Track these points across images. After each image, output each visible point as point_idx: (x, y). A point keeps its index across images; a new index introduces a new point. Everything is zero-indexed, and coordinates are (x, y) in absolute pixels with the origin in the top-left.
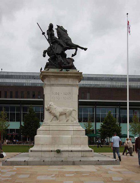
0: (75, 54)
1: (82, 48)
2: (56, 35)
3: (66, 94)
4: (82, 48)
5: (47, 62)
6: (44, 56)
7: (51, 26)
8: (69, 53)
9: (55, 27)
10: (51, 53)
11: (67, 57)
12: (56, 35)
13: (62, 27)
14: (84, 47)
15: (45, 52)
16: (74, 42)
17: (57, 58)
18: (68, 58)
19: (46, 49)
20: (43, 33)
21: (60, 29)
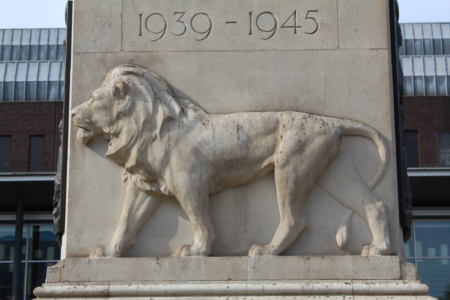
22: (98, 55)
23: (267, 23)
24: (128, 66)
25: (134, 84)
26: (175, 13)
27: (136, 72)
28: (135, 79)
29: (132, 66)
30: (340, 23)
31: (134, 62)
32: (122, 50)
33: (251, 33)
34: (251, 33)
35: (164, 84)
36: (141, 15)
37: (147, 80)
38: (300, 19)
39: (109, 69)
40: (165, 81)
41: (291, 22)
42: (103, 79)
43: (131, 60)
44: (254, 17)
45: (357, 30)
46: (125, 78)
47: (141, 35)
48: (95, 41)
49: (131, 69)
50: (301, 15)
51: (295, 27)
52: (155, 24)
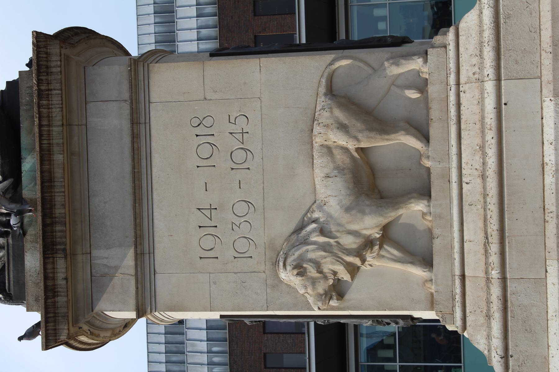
3: (206, 151)
22: (269, 291)
23: (239, 156)
24: (278, 266)
25: (294, 260)
26: (233, 229)
27: (283, 259)
28: (289, 260)
29: (278, 263)
30: (238, 97)
31: (274, 262)
32: (264, 272)
33: (248, 168)
34: (248, 168)
35: (292, 237)
36: (235, 258)
37: (290, 250)
39: (281, 281)
40: (290, 236)
41: (239, 136)
42: (289, 286)
43: (273, 264)
44: (235, 166)
45: (245, 83)
46: (289, 268)
47: (251, 257)
48: (257, 294)
49: (281, 264)
51: (243, 133)
52: (242, 245)
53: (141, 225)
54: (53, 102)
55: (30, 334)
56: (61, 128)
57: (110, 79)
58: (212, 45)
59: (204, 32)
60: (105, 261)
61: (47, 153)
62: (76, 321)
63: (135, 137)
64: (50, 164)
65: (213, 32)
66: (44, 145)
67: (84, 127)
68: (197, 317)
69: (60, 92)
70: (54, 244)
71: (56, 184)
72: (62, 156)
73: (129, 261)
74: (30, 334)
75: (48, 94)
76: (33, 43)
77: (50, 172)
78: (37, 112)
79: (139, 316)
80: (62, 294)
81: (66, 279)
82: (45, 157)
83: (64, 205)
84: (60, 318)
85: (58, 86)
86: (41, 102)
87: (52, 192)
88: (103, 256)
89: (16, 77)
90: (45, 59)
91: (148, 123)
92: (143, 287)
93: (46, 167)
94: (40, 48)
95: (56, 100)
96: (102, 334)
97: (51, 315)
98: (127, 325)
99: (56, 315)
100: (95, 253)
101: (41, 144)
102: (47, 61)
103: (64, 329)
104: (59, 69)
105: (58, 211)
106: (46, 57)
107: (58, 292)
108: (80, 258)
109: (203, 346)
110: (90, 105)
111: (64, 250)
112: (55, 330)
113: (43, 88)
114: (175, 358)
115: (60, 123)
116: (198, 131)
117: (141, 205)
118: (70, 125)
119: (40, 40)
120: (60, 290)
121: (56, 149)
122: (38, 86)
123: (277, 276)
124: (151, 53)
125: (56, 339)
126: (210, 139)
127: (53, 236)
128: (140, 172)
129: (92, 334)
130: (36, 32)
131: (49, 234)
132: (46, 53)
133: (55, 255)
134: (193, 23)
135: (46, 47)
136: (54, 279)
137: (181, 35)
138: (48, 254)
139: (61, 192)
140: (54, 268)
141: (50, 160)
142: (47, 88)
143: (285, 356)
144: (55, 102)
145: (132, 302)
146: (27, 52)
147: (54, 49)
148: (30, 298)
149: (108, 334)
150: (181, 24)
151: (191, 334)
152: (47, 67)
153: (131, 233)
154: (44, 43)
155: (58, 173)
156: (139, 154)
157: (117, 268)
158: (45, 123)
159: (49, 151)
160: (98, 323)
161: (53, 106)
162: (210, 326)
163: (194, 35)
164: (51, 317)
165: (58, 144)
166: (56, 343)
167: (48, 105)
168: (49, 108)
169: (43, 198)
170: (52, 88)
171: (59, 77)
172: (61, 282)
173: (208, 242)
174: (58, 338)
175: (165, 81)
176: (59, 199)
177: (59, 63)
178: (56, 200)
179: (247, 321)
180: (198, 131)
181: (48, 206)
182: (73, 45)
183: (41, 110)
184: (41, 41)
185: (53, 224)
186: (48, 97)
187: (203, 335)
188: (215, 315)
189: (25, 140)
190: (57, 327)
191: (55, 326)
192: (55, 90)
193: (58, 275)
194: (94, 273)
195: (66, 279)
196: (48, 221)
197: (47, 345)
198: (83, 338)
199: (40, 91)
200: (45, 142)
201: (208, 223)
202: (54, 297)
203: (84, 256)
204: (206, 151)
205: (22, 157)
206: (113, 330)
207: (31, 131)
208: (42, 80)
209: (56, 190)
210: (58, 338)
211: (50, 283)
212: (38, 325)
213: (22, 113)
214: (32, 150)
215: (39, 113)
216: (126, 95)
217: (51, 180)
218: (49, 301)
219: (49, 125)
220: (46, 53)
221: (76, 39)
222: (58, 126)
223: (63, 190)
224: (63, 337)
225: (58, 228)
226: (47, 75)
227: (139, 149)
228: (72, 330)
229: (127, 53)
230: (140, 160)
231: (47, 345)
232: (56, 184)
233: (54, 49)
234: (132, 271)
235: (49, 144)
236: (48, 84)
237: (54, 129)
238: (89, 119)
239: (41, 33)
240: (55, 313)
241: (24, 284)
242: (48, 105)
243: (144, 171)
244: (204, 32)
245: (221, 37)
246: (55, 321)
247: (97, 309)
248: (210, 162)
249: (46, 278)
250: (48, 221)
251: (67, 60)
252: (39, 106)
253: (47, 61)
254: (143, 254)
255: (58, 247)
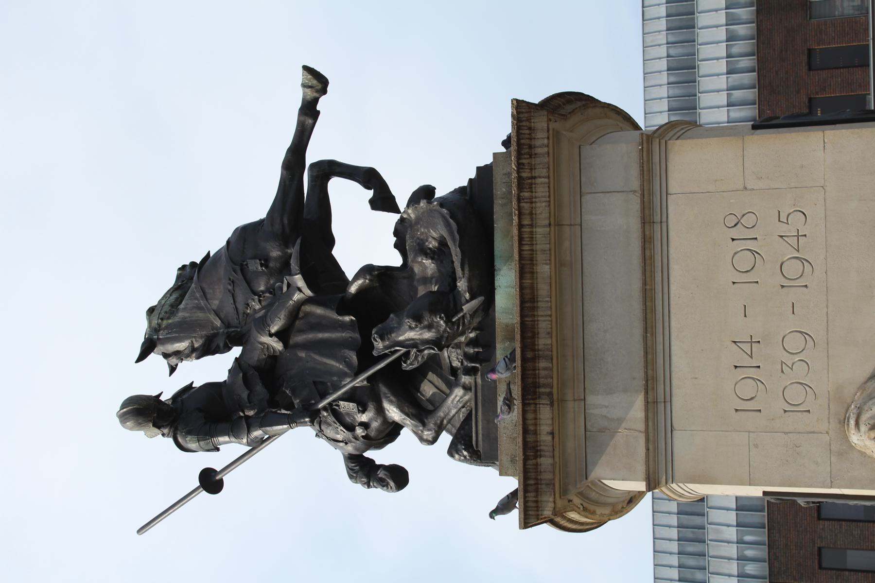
0: (369, 178)
1: (309, 111)
2: (215, 368)
3: (745, 261)
4: (309, 111)
5: (452, 451)
6: (398, 477)
7: (144, 411)
8: (362, 240)
9: (160, 380)
10: (364, 418)
11: (395, 260)
12: (215, 368)
13: (151, 311)
14: (296, 98)
15: (363, 470)
16: (256, 201)
17: (398, 361)
18: (400, 245)
19: (333, 459)
20: (210, 481)
21: (171, 326)
22: (833, 459)
23: (793, 268)
24: (848, 425)
25: (871, 418)
26: (782, 371)
27: (855, 416)
28: (865, 417)
29: (848, 421)
30: (793, 185)
31: (842, 418)
32: (827, 433)
33: (806, 286)
34: (806, 286)
35: (869, 384)
36: (785, 411)
37: (865, 403)
38: (783, 229)
39: (851, 447)
40: (866, 382)
41: (793, 241)
42: (863, 454)
43: (840, 423)
44: (786, 283)
45: (802, 166)
46: (863, 428)
47: (809, 411)
48: (816, 463)
49: (852, 422)
50: (783, 229)
51: (798, 236)
52: (795, 394)
53: (654, 362)
54: (537, 194)
55: (504, 507)
56: (548, 229)
57: (613, 163)
58: (750, 112)
59: (738, 94)
60: (604, 411)
61: (528, 262)
62: (564, 492)
63: (647, 241)
64: (532, 278)
65: (751, 94)
66: (526, 253)
67: (578, 228)
68: (724, 492)
69: (547, 180)
70: (536, 385)
71: (540, 304)
72: (548, 267)
73: (637, 411)
74: (504, 507)
75: (531, 184)
76: (513, 115)
77: (532, 288)
78: (516, 207)
79: (650, 488)
80: (547, 454)
81: (552, 433)
82: (526, 269)
83: (550, 334)
84: (543, 486)
85: (544, 172)
86: (522, 194)
87: (534, 316)
88: (601, 404)
89: (489, 160)
90: (527, 136)
91: (665, 222)
92: (656, 449)
93: (527, 282)
94: (521, 121)
95: (541, 191)
96: (599, 511)
97: (532, 482)
98: (632, 499)
99: (538, 481)
100: (591, 399)
101: (520, 251)
102: (530, 139)
103: (548, 502)
104: (546, 149)
105: (543, 342)
106: (530, 134)
107: (540, 450)
108: (570, 405)
109: (731, 533)
110: (587, 198)
111: (550, 394)
112: (537, 502)
113: (524, 175)
114: (691, 548)
115: (547, 222)
116: (734, 233)
117: (654, 334)
118: (559, 225)
119: (522, 110)
120: (543, 448)
121: (540, 257)
122: (518, 172)
123: (846, 439)
124: (670, 126)
125: (538, 515)
126: (751, 245)
127: (535, 374)
128: (653, 290)
129: (585, 509)
130: (517, 100)
131: (531, 372)
132: (530, 129)
133: (537, 401)
134: (722, 82)
135: (529, 120)
136: (535, 433)
137: (705, 100)
138: (528, 399)
139: (546, 316)
140: (536, 419)
141: (532, 273)
142: (529, 175)
143: (850, 553)
144: (540, 194)
145: (641, 468)
146: (506, 128)
147: (540, 122)
148: (504, 457)
149: (607, 511)
150: (705, 83)
151: (715, 516)
152: (530, 147)
153: (640, 374)
154: (526, 115)
155: (543, 290)
156: (653, 265)
157: (620, 421)
158: (526, 222)
159: (531, 260)
160: (593, 496)
161: (537, 200)
162: (743, 505)
163: (722, 99)
164: (531, 485)
165: (543, 251)
166: (538, 519)
167: (531, 198)
168: (532, 203)
169: (523, 324)
170: (537, 175)
171: (546, 160)
172: (545, 438)
173: (747, 389)
174: (540, 513)
175: (687, 163)
176: (543, 325)
177: (546, 141)
178: (540, 326)
179: (801, 501)
180: (734, 233)
181: (530, 335)
182: (564, 117)
183: (522, 204)
184: (522, 113)
185: (534, 359)
186: (531, 188)
187: (731, 517)
188: (756, 492)
189: (500, 245)
190: (539, 499)
191: (537, 496)
192: (540, 177)
193: (542, 428)
194: (588, 427)
195: (552, 433)
196: (529, 355)
197: (526, 523)
198: (573, 515)
199: (520, 179)
200: (526, 248)
201: (748, 362)
202: (536, 457)
203: (576, 403)
204: (745, 261)
205: (496, 268)
206: (613, 505)
207: (507, 234)
208: (523, 164)
209: (540, 313)
210: (540, 513)
211: (531, 438)
212: (514, 494)
213: (496, 208)
214: (510, 258)
215: (520, 209)
216: (635, 184)
217: (534, 299)
218: (530, 462)
219: (531, 226)
220: (530, 129)
221: (569, 108)
222: (544, 226)
223: (549, 313)
224: (547, 513)
225: (542, 364)
226: (531, 157)
227: (652, 257)
228: (560, 503)
229: (636, 127)
230: (653, 273)
231: (526, 523)
232: (540, 304)
233: (540, 122)
234: (641, 426)
235: (532, 250)
236: (531, 169)
237: (539, 230)
238: (585, 217)
239: (523, 101)
240: (537, 479)
241: (496, 439)
242: (531, 198)
243: (658, 288)
244: (738, 94)
245: (762, 102)
246: (537, 491)
247: (593, 476)
248: (751, 277)
249: (525, 431)
250: (529, 355)
251: (556, 136)
252: (519, 200)
253: (530, 139)
254: (656, 402)
255: (542, 390)
